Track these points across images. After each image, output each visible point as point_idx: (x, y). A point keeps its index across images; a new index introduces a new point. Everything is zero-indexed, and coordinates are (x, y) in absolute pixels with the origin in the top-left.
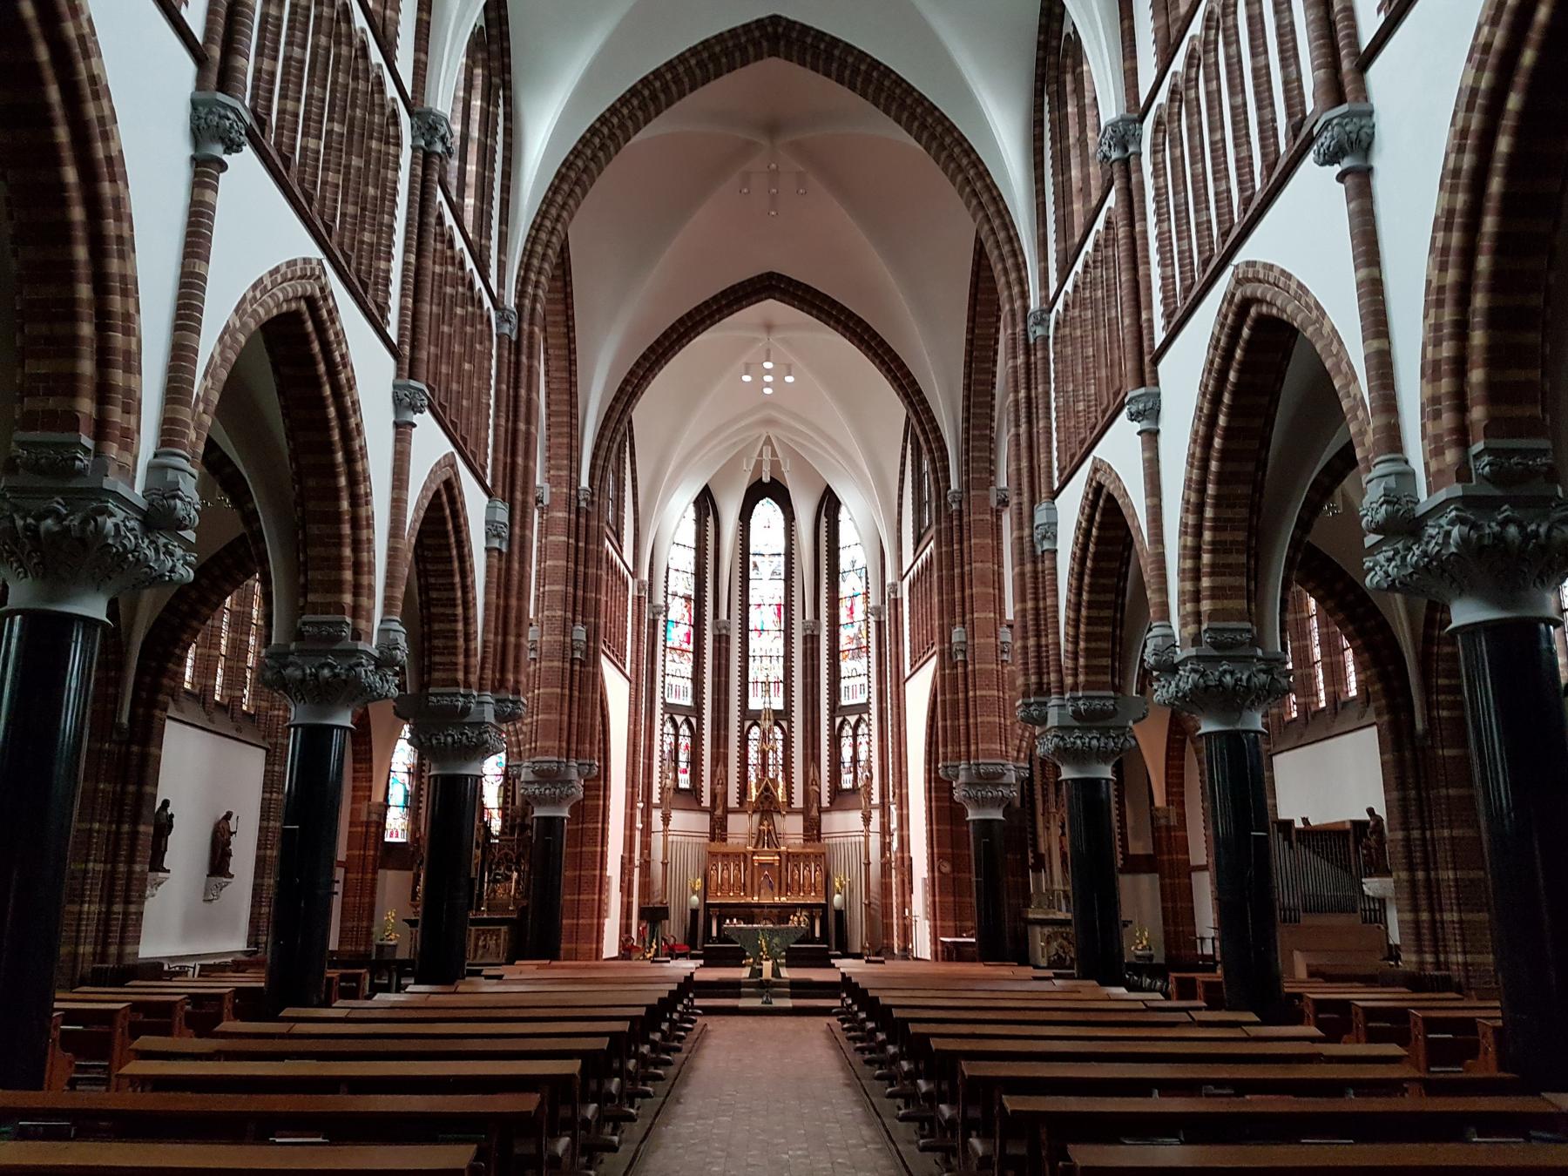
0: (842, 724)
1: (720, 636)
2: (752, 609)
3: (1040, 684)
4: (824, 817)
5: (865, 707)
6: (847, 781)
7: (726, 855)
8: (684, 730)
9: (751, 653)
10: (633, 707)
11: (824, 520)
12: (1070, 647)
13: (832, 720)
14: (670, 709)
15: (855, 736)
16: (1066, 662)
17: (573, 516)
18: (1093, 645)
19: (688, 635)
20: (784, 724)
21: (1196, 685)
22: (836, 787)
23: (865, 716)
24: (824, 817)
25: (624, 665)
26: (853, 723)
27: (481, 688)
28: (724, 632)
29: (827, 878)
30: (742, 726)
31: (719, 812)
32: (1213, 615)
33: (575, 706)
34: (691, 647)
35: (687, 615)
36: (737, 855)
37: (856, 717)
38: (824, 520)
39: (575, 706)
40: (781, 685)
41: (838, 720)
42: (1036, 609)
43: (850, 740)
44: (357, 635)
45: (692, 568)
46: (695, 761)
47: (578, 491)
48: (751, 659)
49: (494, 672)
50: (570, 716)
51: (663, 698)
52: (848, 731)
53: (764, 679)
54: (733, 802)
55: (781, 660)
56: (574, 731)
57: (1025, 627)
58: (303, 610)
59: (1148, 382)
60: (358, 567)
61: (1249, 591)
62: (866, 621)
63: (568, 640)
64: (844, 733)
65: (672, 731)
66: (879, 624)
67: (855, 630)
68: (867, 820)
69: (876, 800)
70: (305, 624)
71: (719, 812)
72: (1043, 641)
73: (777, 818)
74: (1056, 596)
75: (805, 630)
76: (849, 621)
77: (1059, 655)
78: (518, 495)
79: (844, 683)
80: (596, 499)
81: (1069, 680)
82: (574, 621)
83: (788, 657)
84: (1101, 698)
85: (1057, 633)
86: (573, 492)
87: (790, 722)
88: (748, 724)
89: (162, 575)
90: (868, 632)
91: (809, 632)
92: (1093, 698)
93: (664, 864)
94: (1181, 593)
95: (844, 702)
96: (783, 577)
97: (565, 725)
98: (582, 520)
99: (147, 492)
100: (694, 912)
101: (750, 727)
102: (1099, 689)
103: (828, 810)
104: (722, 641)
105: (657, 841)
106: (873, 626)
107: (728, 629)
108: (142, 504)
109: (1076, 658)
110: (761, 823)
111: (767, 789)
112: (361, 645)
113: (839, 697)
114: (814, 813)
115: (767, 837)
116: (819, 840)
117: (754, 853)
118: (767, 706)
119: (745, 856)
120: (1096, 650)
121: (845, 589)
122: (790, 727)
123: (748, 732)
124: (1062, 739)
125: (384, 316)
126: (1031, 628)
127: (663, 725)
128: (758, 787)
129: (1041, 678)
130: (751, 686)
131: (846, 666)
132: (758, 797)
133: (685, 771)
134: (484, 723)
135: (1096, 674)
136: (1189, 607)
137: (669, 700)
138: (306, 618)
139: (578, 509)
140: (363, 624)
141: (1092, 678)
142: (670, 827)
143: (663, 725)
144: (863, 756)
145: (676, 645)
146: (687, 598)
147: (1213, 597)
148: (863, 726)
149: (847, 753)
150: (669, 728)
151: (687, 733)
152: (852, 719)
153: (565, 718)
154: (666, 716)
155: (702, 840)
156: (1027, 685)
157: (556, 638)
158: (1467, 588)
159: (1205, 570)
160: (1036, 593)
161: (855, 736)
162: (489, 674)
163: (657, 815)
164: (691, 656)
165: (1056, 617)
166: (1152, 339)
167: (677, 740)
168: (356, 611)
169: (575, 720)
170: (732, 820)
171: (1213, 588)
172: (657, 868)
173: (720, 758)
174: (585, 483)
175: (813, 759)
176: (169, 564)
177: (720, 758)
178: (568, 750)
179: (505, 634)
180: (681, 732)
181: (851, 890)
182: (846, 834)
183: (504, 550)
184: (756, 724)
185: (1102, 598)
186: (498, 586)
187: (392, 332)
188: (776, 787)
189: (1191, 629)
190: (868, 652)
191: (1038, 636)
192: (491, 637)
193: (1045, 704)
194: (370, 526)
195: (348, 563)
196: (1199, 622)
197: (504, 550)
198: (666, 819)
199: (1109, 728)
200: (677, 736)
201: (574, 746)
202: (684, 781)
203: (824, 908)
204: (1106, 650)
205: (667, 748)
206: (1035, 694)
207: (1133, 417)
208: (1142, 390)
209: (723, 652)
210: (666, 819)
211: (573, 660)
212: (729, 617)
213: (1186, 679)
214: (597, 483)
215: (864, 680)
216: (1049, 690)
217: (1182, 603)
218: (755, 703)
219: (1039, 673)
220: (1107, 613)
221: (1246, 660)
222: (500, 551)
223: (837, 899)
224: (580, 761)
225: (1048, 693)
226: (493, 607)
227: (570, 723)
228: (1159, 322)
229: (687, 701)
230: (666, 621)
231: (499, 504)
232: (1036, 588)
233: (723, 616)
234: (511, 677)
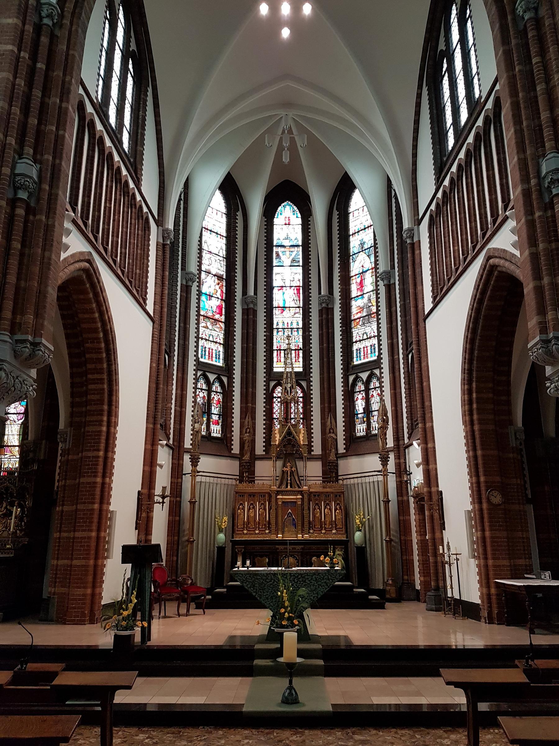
0: (355, 381)
1: (248, 309)
2: (275, 291)
4: (341, 462)
5: (377, 363)
6: (360, 429)
7: (252, 495)
8: (216, 387)
11: (336, 213)
19: (220, 307)
20: (304, 384)
22: (351, 434)
23: (377, 372)
24: (341, 462)
25: (145, 300)
28: (251, 306)
29: (347, 515)
30: (267, 385)
31: (247, 457)
34: (223, 318)
35: (219, 291)
37: (367, 374)
38: (336, 213)
40: (301, 352)
41: (351, 378)
45: (223, 253)
51: (196, 356)
52: (360, 386)
53: (284, 346)
54: (260, 449)
62: (376, 291)
64: (357, 389)
65: (204, 387)
66: (390, 288)
67: (365, 300)
68: (384, 461)
69: (390, 443)
71: (247, 457)
75: (320, 304)
76: (359, 293)
79: (355, 347)
83: (306, 328)
87: (309, 382)
88: (272, 384)
90: (377, 302)
91: (324, 305)
93: (193, 503)
95: (356, 362)
96: (301, 264)
100: (221, 550)
101: (275, 387)
103: (344, 456)
105: (187, 482)
106: (382, 290)
107: (255, 304)
110: (284, 465)
111: (289, 433)
113: (352, 358)
114: (332, 457)
116: (337, 480)
117: (278, 493)
119: (270, 496)
121: (355, 268)
122: (309, 386)
123: (273, 391)
128: (281, 432)
130: (275, 353)
131: (357, 333)
132: (281, 441)
133: (217, 423)
142: (198, 468)
145: (210, 314)
146: (220, 277)
148: (374, 380)
149: (360, 405)
150: (202, 384)
151: (219, 390)
152: (364, 376)
154: (199, 373)
155: (234, 482)
163: (187, 458)
164: (223, 325)
167: (209, 395)
170: (258, 464)
172: (186, 506)
175: (330, 411)
180: (214, 388)
181: (371, 528)
182: (362, 475)
184: (279, 384)
188: (298, 432)
190: (378, 319)
198: (195, 461)
200: (209, 391)
202: (216, 430)
203: (345, 544)
209: (251, 323)
210: (195, 461)
212: (255, 293)
215: (375, 341)
218: (278, 367)
223: (358, 535)
229: (220, 363)
230: (200, 293)
233: (251, 292)
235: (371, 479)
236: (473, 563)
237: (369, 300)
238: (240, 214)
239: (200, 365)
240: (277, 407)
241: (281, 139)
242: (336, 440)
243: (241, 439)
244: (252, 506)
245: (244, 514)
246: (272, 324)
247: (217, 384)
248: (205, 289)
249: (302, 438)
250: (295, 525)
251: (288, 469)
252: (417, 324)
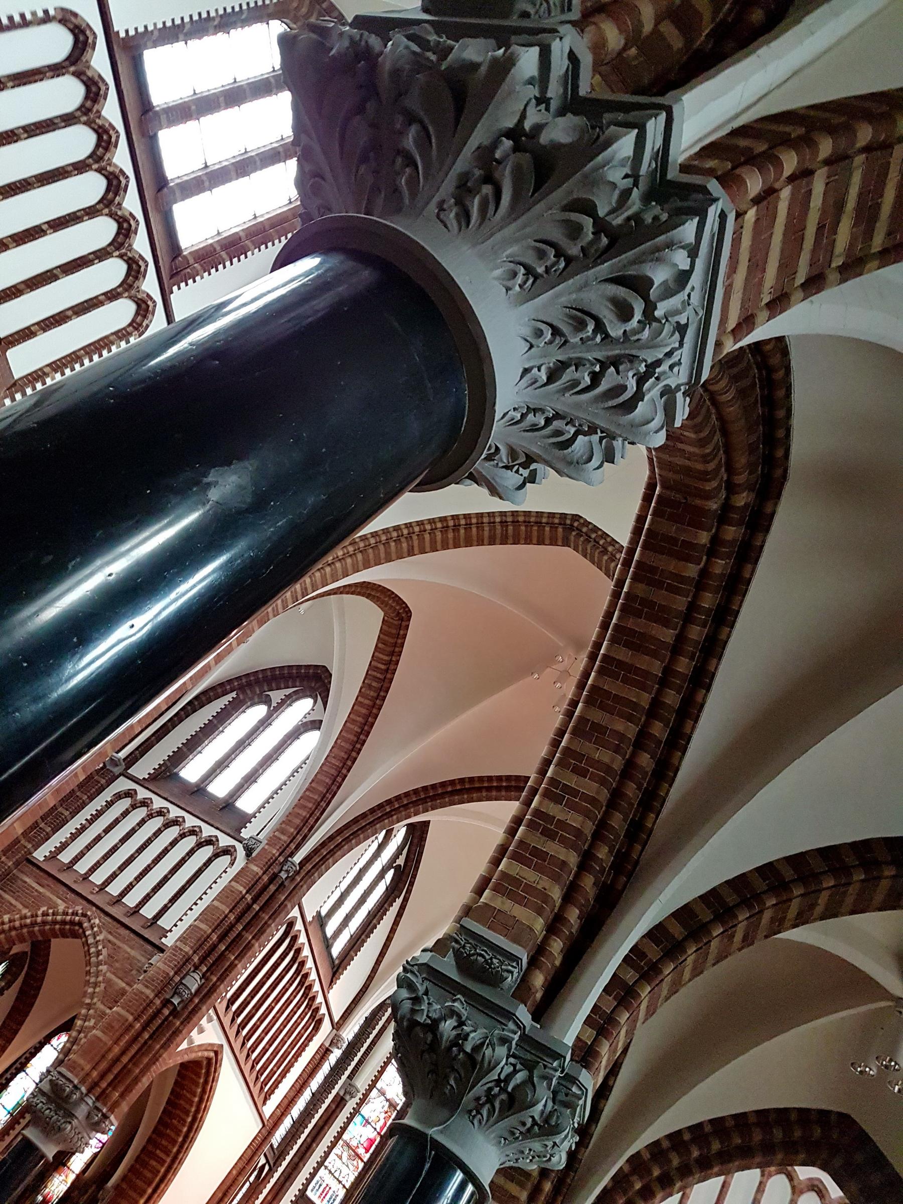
10: (250, 1152)
17: (266, 878)
33: (136, 1047)
39: (136, 1047)
47: (286, 860)
50: (123, 1052)
56: (116, 1071)
63: (177, 979)
80: (298, 879)
82: (196, 968)
86: (281, 859)
97: (110, 1056)
98: (272, 888)
104: (340, 1102)
139: (275, 876)
153: (117, 1050)
157: (167, 969)
169: (125, 1059)
174: (298, 858)
178: (96, 1084)
201: (104, 1085)
211: (167, 1002)
214: (309, 866)
224: (98, 1105)
227: (117, 1059)
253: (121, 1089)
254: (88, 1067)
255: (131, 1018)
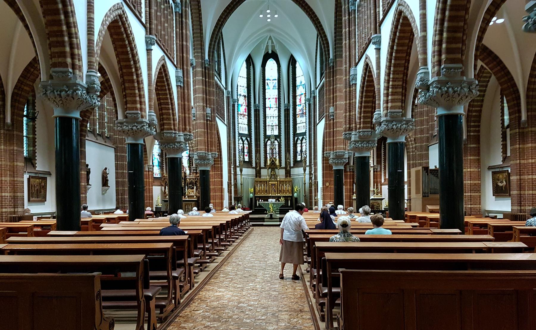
2: (267, 100)
3: (350, 127)
5: (304, 134)
6: (299, 158)
7: (261, 182)
8: (246, 142)
9: (267, 116)
11: (291, 67)
12: (359, 116)
13: (294, 138)
14: (241, 135)
15: (301, 143)
16: (357, 120)
17: (204, 70)
18: (365, 115)
19: (245, 109)
20: (278, 140)
21: (385, 128)
23: (305, 137)
24: (292, 170)
25: (224, 120)
26: (301, 139)
27: (179, 131)
28: (258, 108)
30: (265, 141)
31: (258, 168)
32: (392, 107)
33: (209, 135)
34: (247, 114)
35: (245, 102)
36: (264, 182)
37: (302, 137)
38: (291, 67)
40: (277, 126)
41: (296, 138)
42: (350, 103)
43: (300, 145)
44: (142, 117)
45: (246, 85)
46: (250, 152)
47: (205, 61)
48: (267, 118)
49: (182, 126)
50: (208, 138)
52: (299, 142)
53: (271, 124)
54: (262, 165)
55: (277, 118)
57: (346, 109)
58: (126, 109)
59: (378, 32)
60: (140, 96)
61: (402, 100)
63: (205, 113)
64: (298, 143)
65: (242, 142)
66: (310, 105)
67: (301, 107)
68: (305, 170)
69: (308, 164)
70: (127, 113)
71: (258, 168)
72: (351, 114)
73: (276, 170)
74: (356, 99)
75: (285, 107)
76: (300, 104)
77: (356, 118)
78: (185, 67)
79: (298, 126)
80: (211, 63)
81: (358, 126)
82: (206, 107)
84: (367, 132)
85: (355, 111)
86: (203, 61)
87: (280, 139)
88: (266, 140)
89: (93, 105)
91: (286, 108)
92: (365, 132)
93: (241, 184)
94: (384, 101)
95: (298, 132)
96: (277, 88)
97: (206, 141)
98: (207, 71)
99: (87, 83)
100: (251, 199)
101: (267, 141)
102: (367, 129)
103: (293, 167)
104: (257, 111)
105: (239, 177)
106: (307, 105)
107: (259, 107)
108: (86, 86)
109: (360, 119)
110: (271, 172)
112: (144, 120)
113: (296, 130)
114: (288, 168)
115: (274, 176)
116: (290, 177)
117: (269, 181)
118: (272, 134)
120: (366, 116)
121: (298, 92)
122: (280, 141)
123: (267, 143)
124: (355, 144)
125: (140, 15)
126: (348, 110)
127: (239, 140)
128: (270, 160)
129: (350, 126)
130: (267, 127)
131: (299, 120)
132: (270, 164)
133: (247, 156)
134: (181, 142)
135: (366, 124)
136: (385, 105)
137: (240, 132)
138: (127, 112)
139: (205, 67)
140: (143, 113)
141: (365, 125)
143: (239, 140)
144: (304, 150)
145: (242, 113)
146: (245, 96)
147: (391, 102)
149: (299, 149)
150: (241, 141)
151: (247, 143)
152: (301, 138)
153: (206, 139)
154: (240, 137)
155: (253, 177)
156: (346, 128)
157: (201, 112)
158: (438, 105)
159: (390, 94)
160: (350, 98)
161: (301, 143)
162: (181, 126)
163: (238, 169)
164: (247, 117)
165: (355, 106)
166: (379, 18)
167: (243, 145)
168: (141, 109)
169: (209, 140)
170: (262, 170)
171: (391, 99)
172: (239, 185)
173: (258, 151)
175: (288, 151)
176: (94, 101)
177: (258, 151)
178: (208, 149)
179: (185, 114)
180: (245, 143)
181: (300, 192)
182: (299, 175)
183: (182, 85)
184: (269, 140)
185: (368, 99)
186: (181, 98)
187: (143, 20)
188: (276, 160)
189: (385, 112)
191: (350, 112)
192: (181, 114)
193: (351, 134)
194: (142, 83)
195: (137, 95)
196: (388, 110)
197: (182, 85)
198: (241, 171)
199: (369, 141)
200: (243, 144)
201: (209, 148)
202: (247, 159)
203: (292, 197)
204: (370, 116)
205: (240, 148)
206: (348, 131)
207: (374, 43)
208: (376, 35)
209: (258, 115)
210: (241, 171)
211: (207, 120)
212: (259, 103)
213: (383, 126)
215: (304, 124)
216: (352, 129)
217: (384, 104)
218: (269, 133)
219: (350, 124)
220: (370, 104)
221: (401, 121)
222: (181, 86)
223: (295, 195)
224: (212, 153)
225: (352, 130)
226: (180, 105)
227: (208, 141)
228: (381, 13)
230: (238, 105)
231: (179, 70)
232: (350, 96)
233: (257, 103)
234: (188, 127)
235: (301, 176)
236: (322, 201)
237: (303, 107)
238: (252, 67)
239: (240, 134)
240: (268, 148)
241: (268, 43)
242: (290, 162)
243: (256, 162)
244: (261, 185)
245: (258, 188)
246: (266, 115)
247: (246, 141)
248: (240, 103)
249: (277, 163)
250: (275, 191)
251: (273, 173)
252: (314, 126)
253: (214, 146)
254: (204, 147)
255: (203, 130)
